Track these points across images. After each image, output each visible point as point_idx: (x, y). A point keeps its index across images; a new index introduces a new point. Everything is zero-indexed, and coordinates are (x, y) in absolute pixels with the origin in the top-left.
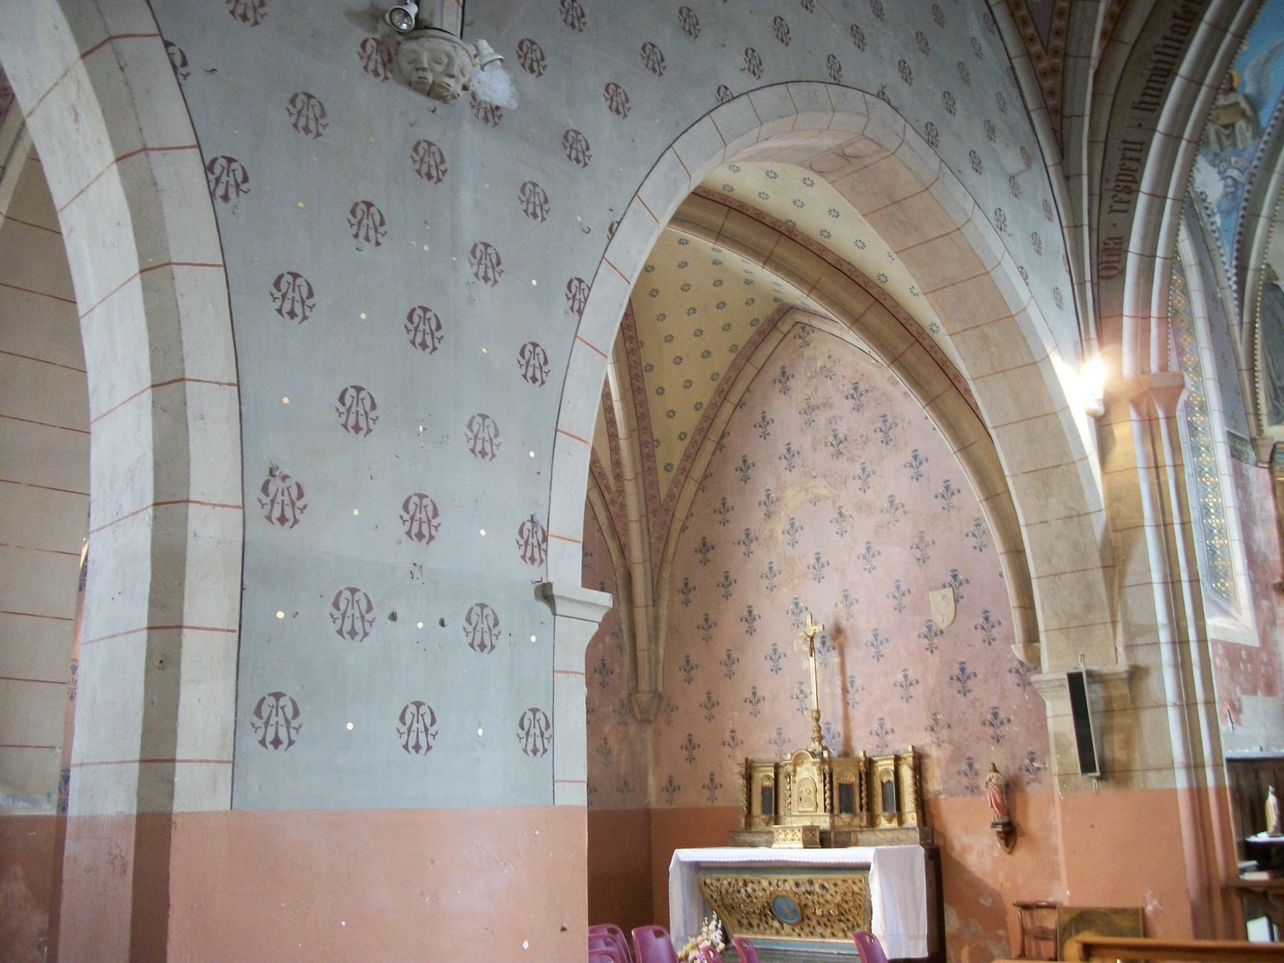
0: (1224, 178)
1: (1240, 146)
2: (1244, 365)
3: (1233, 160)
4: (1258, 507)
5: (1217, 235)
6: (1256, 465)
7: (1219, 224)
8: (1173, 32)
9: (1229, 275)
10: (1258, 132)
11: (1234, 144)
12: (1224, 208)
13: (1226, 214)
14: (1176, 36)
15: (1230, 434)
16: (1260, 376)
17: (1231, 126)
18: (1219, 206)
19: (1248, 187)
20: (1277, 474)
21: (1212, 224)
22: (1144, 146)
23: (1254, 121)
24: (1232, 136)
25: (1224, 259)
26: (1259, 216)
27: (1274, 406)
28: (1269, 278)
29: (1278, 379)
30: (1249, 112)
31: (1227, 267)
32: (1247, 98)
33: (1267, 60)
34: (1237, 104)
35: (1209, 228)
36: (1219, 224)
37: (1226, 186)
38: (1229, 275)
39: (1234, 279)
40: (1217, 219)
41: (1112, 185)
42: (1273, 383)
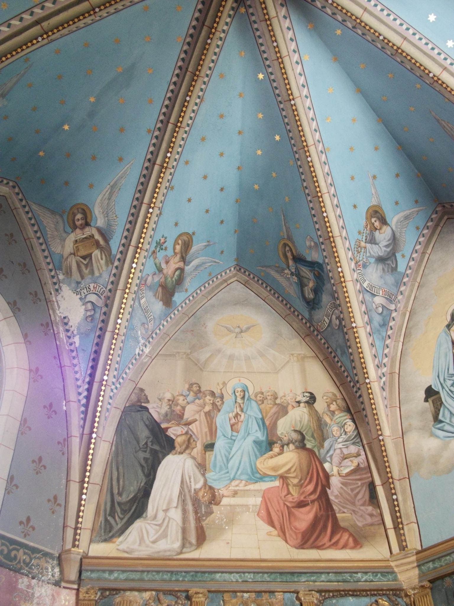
0: (85, 304)
1: (97, 274)
3: (92, 286)
5: (74, 354)
6: (57, 584)
7: (77, 345)
10: (110, 261)
11: (92, 272)
13: (84, 335)
17: (89, 256)
18: (78, 329)
19: (104, 309)
21: (71, 344)
23: (106, 250)
25: (78, 376)
27: (106, 520)
28: (139, 401)
29: (120, 494)
30: (102, 242)
31: (79, 383)
32: (99, 230)
33: (111, 194)
36: (77, 345)
37: (86, 310)
38: (80, 390)
40: (77, 340)
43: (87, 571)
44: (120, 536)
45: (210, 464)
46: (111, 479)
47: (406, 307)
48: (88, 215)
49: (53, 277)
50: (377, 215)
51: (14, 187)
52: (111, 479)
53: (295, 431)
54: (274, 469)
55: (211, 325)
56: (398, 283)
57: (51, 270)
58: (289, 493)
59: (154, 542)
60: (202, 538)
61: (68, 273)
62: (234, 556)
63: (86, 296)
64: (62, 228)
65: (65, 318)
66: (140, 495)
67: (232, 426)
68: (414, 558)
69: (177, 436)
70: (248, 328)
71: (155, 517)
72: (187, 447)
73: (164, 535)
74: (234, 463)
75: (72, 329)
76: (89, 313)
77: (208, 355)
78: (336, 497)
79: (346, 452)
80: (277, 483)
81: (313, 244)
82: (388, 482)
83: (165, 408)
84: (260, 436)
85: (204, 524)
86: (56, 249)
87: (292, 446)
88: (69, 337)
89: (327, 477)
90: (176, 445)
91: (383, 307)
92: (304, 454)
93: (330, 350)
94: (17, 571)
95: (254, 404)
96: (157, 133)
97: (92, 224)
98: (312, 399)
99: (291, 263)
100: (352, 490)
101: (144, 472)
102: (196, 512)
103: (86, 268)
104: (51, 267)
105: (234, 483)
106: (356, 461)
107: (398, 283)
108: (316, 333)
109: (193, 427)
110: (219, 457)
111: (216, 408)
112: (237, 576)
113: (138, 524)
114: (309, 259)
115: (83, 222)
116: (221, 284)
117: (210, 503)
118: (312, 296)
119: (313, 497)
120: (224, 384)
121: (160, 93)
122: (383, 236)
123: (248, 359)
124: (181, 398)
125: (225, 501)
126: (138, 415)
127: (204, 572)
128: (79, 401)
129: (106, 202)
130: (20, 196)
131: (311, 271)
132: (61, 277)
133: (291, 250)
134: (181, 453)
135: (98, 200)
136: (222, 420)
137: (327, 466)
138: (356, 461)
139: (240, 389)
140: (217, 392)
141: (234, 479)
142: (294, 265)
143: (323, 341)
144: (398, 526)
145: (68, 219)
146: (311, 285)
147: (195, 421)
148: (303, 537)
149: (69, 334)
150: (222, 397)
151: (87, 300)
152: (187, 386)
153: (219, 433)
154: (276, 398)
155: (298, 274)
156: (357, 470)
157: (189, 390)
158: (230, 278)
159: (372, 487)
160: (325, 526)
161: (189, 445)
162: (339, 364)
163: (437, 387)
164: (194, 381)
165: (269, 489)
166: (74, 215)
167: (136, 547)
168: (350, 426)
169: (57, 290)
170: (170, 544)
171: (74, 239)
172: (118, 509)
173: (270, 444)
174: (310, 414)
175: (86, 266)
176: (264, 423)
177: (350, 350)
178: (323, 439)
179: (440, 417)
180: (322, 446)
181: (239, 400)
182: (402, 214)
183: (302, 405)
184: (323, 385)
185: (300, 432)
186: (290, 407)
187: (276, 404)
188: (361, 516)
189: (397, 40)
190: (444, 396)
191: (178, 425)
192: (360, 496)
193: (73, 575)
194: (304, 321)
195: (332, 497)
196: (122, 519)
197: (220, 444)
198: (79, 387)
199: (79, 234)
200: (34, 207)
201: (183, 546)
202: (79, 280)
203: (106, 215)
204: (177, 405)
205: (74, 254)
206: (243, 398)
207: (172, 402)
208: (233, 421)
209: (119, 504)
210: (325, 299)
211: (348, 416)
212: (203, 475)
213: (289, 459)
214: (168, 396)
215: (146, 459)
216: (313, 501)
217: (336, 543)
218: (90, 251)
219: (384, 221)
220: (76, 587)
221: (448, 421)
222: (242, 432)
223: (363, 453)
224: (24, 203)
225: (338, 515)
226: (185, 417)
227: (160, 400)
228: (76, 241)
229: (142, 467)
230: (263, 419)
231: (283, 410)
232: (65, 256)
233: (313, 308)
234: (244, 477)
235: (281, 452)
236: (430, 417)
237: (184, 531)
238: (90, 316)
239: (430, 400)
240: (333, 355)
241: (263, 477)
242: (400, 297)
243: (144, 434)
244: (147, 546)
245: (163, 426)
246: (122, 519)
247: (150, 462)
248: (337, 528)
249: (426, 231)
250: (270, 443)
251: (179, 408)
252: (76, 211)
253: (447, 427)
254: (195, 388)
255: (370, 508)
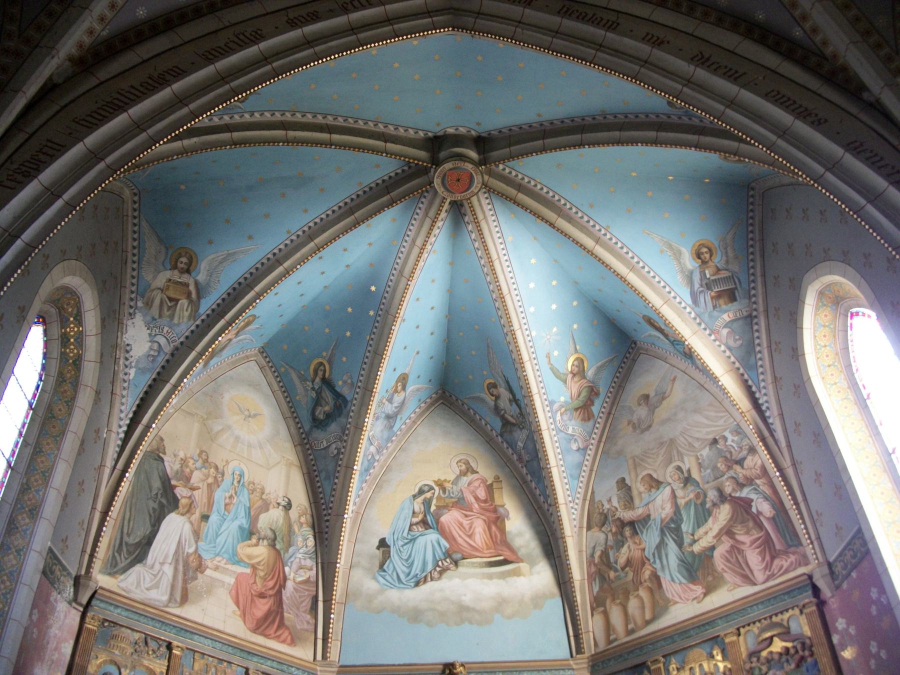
1: (176, 321)
2: (100, 506)
3: (166, 329)
4: (52, 645)
5: (126, 385)
6: (70, 603)
7: (131, 377)
8: (141, 86)
9: (122, 423)
10: (194, 315)
11: (172, 317)
12: (141, 366)
13: (141, 371)
14: (142, 89)
15: (50, 550)
16: (110, 523)
17: (177, 301)
18: (138, 362)
20: (87, 620)
21: (126, 374)
22: (63, 149)
23: (195, 305)
24: (173, 308)
25: (123, 408)
26: (168, 382)
27: (114, 556)
28: (158, 449)
29: (129, 535)
30: (194, 296)
31: (122, 415)
32: (197, 283)
34: (187, 285)
35: (121, 375)
36: (131, 377)
37: (151, 349)
38: (122, 423)
39: (125, 428)
40: (132, 372)
41: (15, 166)
42: (122, 538)
43: (98, 599)
44: (122, 574)
45: (203, 535)
46: (124, 519)
47: (385, 461)
48: (193, 264)
49: (132, 299)
50: (403, 380)
51: (135, 194)
52: (124, 519)
53: (271, 529)
54: (250, 557)
55: (227, 397)
56: (389, 440)
57: (132, 292)
58: (255, 582)
59: (148, 589)
60: (184, 599)
61: (149, 304)
62: (206, 623)
63: (156, 335)
64: (162, 260)
65: (128, 345)
66: (144, 541)
67: (226, 505)
68: (336, 669)
69: (183, 497)
70: (255, 415)
71: (152, 567)
72: (188, 511)
73: (156, 586)
74: (221, 540)
75: (131, 360)
76: (152, 353)
77: (220, 428)
78: (287, 598)
79: (303, 562)
80: (248, 571)
81: (349, 381)
82: (328, 601)
83: (177, 467)
84: (244, 522)
85: (189, 586)
86: (147, 275)
87: (265, 542)
88: (126, 366)
89: (285, 579)
90: (180, 505)
91: (373, 456)
92: (273, 551)
93: (315, 468)
94: (52, 584)
95: (246, 492)
96: (294, 237)
97: (193, 274)
98: (288, 506)
99: (318, 380)
100: (300, 597)
101: (150, 520)
102: (185, 574)
103: (168, 310)
104: (134, 288)
105: (218, 559)
106: (308, 574)
107: (389, 440)
108: (308, 446)
109: (196, 493)
110: (210, 531)
111: (217, 483)
112: (210, 641)
113: (138, 568)
114: (338, 390)
115: (186, 267)
116: (243, 358)
117: (197, 570)
118: (321, 417)
119: (271, 592)
120: (227, 462)
121: (318, 210)
122: (398, 399)
123: (250, 446)
124: (192, 462)
125: (208, 572)
126: (155, 464)
127: (186, 631)
128: (118, 433)
129: (216, 263)
130: (136, 206)
131: (334, 399)
132: (140, 304)
133: (325, 371)
134: (183, 515)
135: (210, 258)
136: (220, 495)
137: (287, 569)
138: (308, 574)
139: (238, 473)
140: (220, 467)
141: (218, 555)
142: (320, 384)
143: (311, 457)
144: (325, 639)
145: (172, 255)
146: (327, 408)
147: (198, 488)
148: (257, 624)
149: (127, 363)
150: (223, 475)
151: (156, 339)
152: (198, 451)
153: (215, 508)
154: (263, 493)
155: (319, 393)
156: (307, 581)
157: (200, 455)
158: (251, 356)
159: (315, 600)
160: (272, 620)
161: (189, 510)
162: (319, 484)
163: (389, 542)
164: (204, 448)
165: (242, 574)
166: (180, 256)
167: (133, 588)
168: (311, 542)
169: (130, 314)
170: (159, 596)
171: (168, 277)
172: (125, 549)
173: (251, 534)
174: (285, 519)
175: (169, 308)
176: (249, 512)
177: (336, 481)
178: (289, 545)
179: (385, 567)
180: (287, 551)
181: (235, 483)
182: (417, 386)
183: (281, 507)
184: (300, 497)
185: (274, 532)
186: (271, 506)
187: (261, 498)
188: (301, 621)
189: (505, 291)
190: (393, 550)
191: (185, 486)
192: (304, 604)
193: (84, 601)
194: (301, 431)
195: (284, 598)
196: (126, 559)
197: (214, 518)
198: (121, 419)
199: (176, 276)
200: (144, 223)
201: (170, 600)
202: (157, 317)
203: (211, 275)
204: (187, 466)
205: (162, 291)
206: (239, 482)
207: (184, 462)
208: (228, 500)
209: (126, 543)
210: (334, 427)
211: (312, 532)
212: (196, 542)
213: (261, 552)
214: (182, 455)
215: (153, 508)
216: (270, 596)
217: (279, 636)
218: (178, 297)
219: (404, 388)
220: (82, 609)
221: (390, 572)
222: (232, 514)
223: (315, 569)
224: (136, 214)
225: (285, 614)
226: (192, 481)
227: (175, 455)
228: (170, 280)
229: (150, 516)
230: (249, 508)
231: (265, 507)
232: (153, 286)
233: (317, 427)
234: (226, 556)
235: (257, 545)
236: (377, 564)
237: (173, 587)
238: (153, 356)
239: (382, 549)
240: (316, 473)
241: (239, 562)
242: (385, 451)
243: (157, 484)
244: (142, 591)
245: (173, 482)
246: (126, 559)
247: (157, 513)
248: (282, 624)
249: (423, 405)
250: (250, 533)
251: (188, 470)
252: (183, 254)
253: (388, 577)
254: (204, 457)
255: (309, 617)
